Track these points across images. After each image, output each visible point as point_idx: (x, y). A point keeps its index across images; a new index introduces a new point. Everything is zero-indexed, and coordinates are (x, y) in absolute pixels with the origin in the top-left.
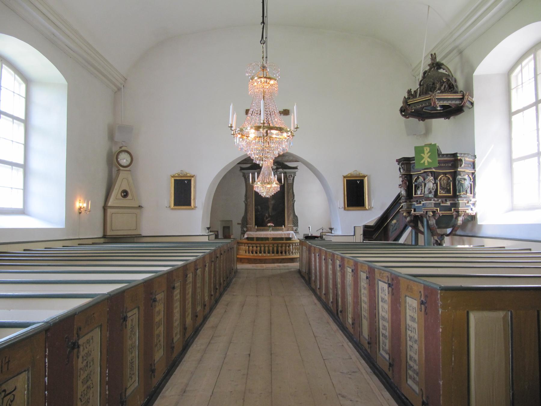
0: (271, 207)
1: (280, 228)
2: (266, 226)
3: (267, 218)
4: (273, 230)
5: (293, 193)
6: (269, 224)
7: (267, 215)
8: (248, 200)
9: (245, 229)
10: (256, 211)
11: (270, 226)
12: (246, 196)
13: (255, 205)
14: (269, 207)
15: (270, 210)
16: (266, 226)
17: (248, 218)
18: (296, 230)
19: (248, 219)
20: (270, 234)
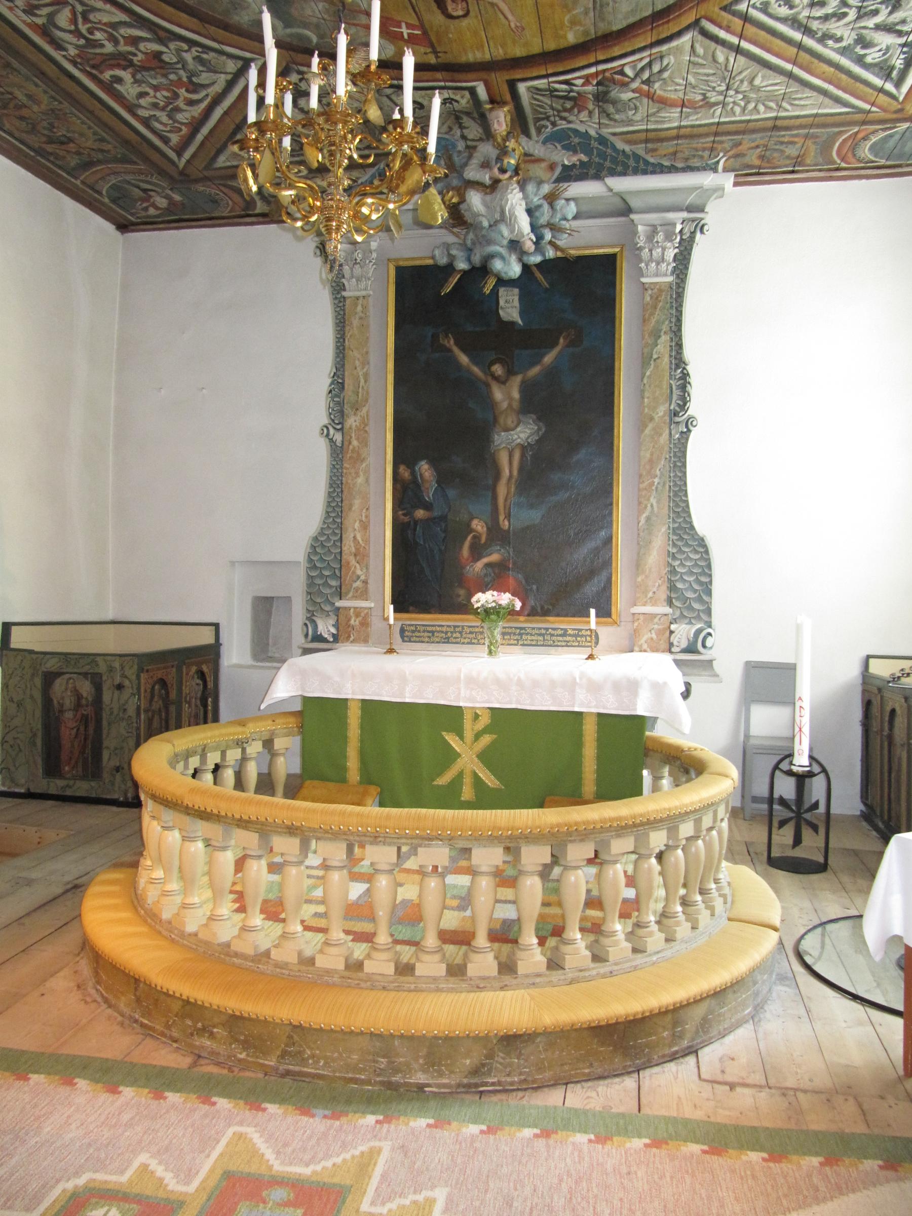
0: (508, 466)
1: (569, 624)
2: (465, 608)
3: (477, 551)
4: (517, 638)
5: (679, 361)
6: (483, 599)
7: (478, 526)
8: (352, 422)
9: (326, 627)
10: (406, 494)
11: (487, 613)
12: (338, 385)
13: (398, 460)
14: (497, 476)
15: (502, 490)
16: (465, 608)
17: (349, 546)
18: (691, 649)
19: (348, 557)
20: (471, 681)
